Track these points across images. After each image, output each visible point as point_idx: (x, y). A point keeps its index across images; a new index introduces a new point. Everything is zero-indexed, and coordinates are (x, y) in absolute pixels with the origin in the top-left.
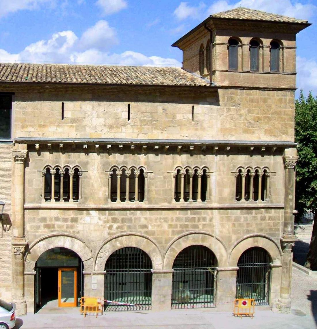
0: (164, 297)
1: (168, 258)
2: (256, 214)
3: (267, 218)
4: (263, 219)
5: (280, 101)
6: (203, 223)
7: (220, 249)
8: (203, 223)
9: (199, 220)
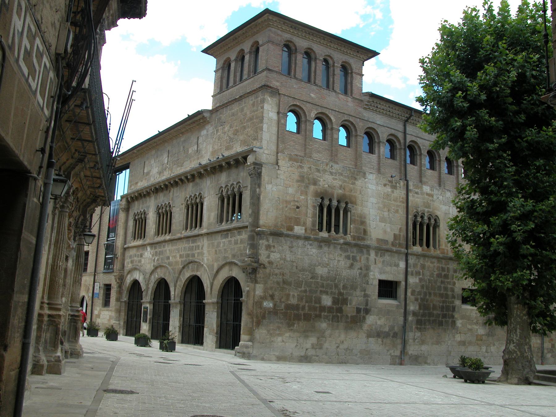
0: (175, 328)
1: (178, 288)
2: (231, 237)
3: (239, 242)
4: (236, 243)
5: (253, 105)
6: (198, 251)
7: (206, 279)
8: (198, 251)
9: (195, 250)
